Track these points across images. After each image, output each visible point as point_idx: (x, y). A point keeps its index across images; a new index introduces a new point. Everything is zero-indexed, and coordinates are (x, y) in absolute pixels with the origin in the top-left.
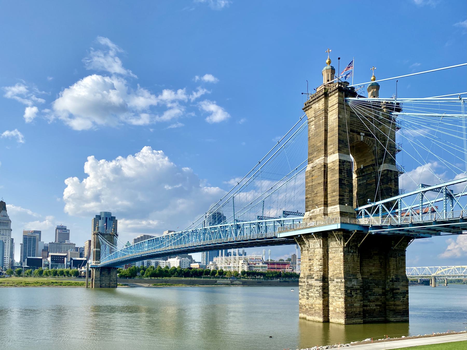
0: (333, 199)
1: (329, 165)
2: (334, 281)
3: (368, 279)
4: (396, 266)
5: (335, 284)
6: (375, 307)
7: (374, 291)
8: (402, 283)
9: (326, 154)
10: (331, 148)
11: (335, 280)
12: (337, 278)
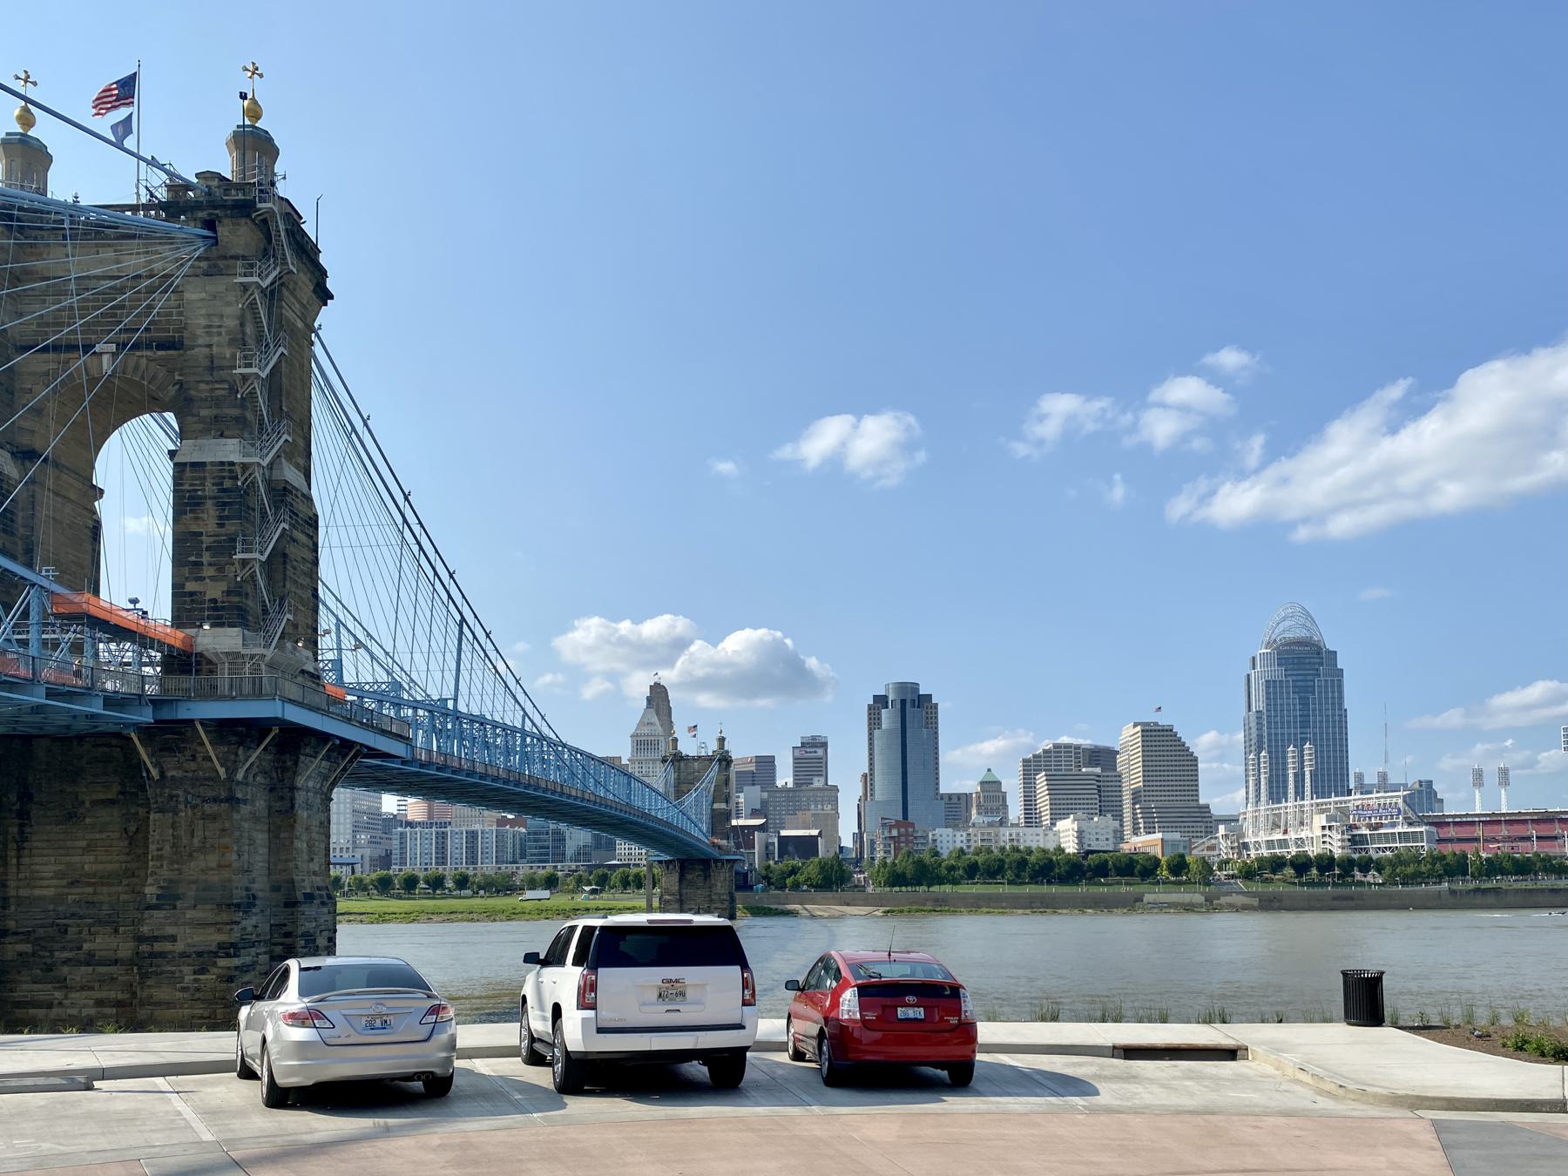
3: (59, 899)
4: (174, 845)
6: (92, 1011)
7: (86, 946)
8: (190, 914)
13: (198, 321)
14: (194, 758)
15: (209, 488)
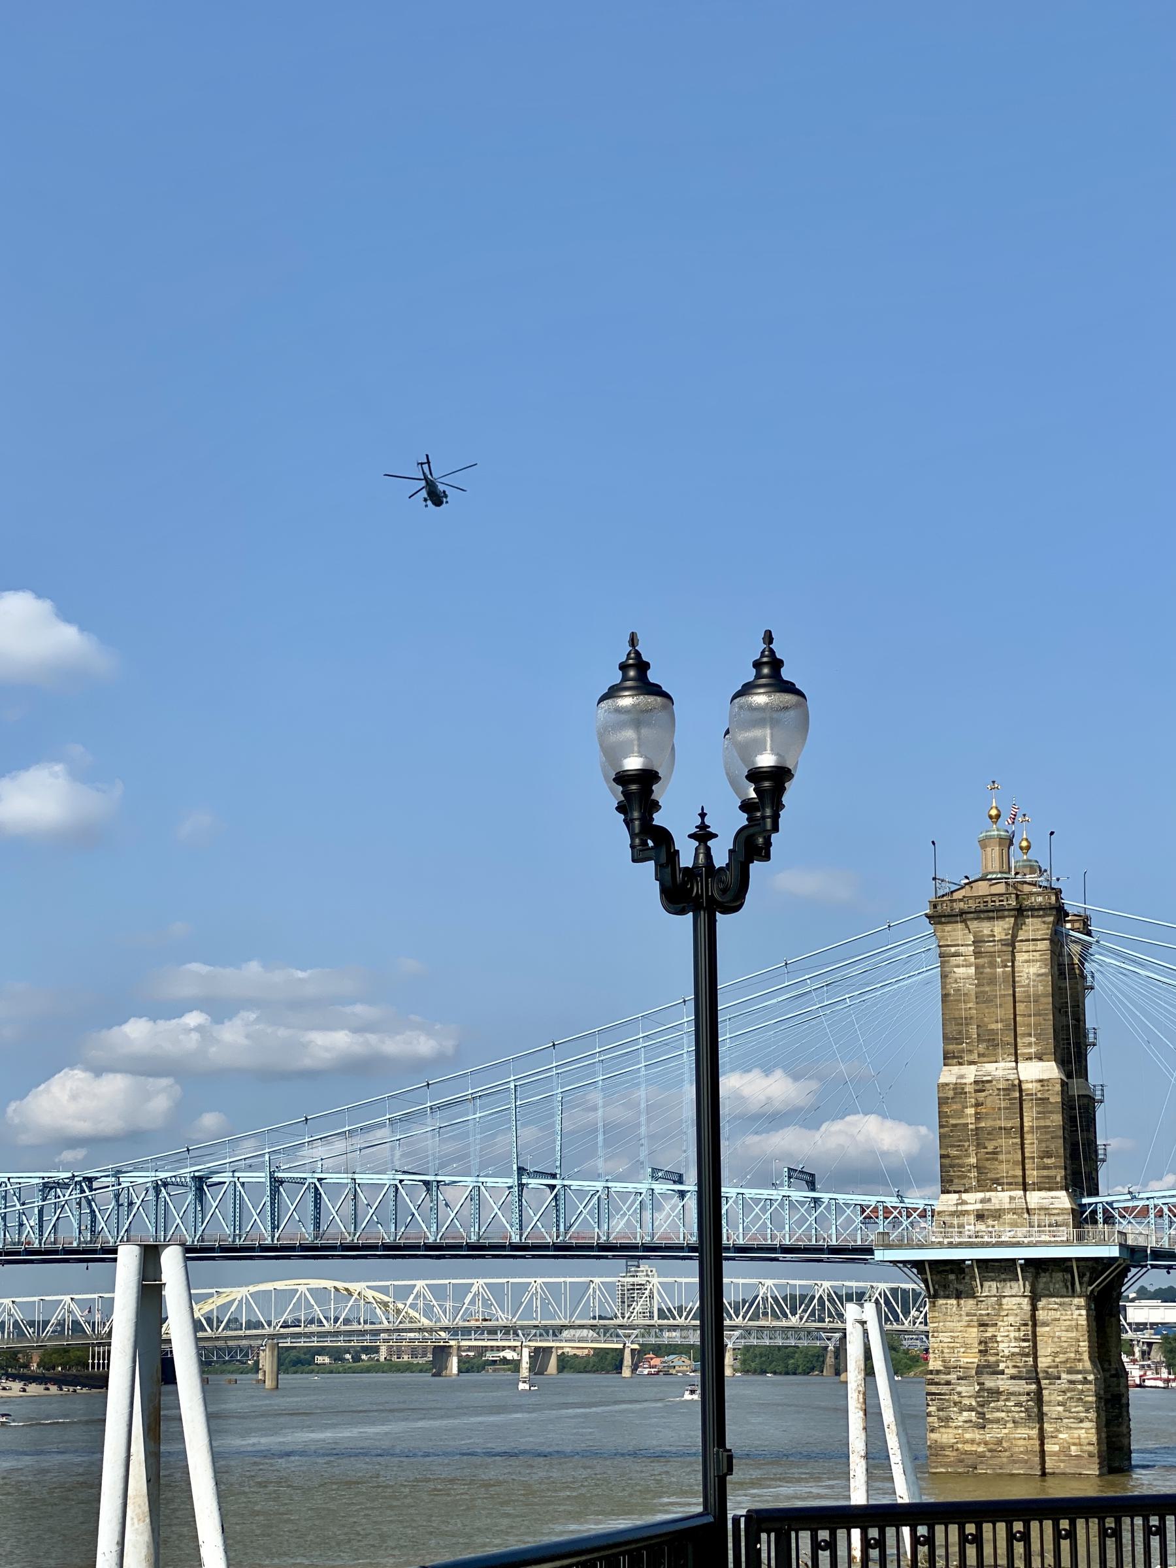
0: (1045, 1173)
1: (1024, 1086)
2: (1059, 1378)
5: (1065, 1386)
9: (1016, 1062)
10: (1030, 1045)
11: (1064, 1376)
12: (1069, 1372)
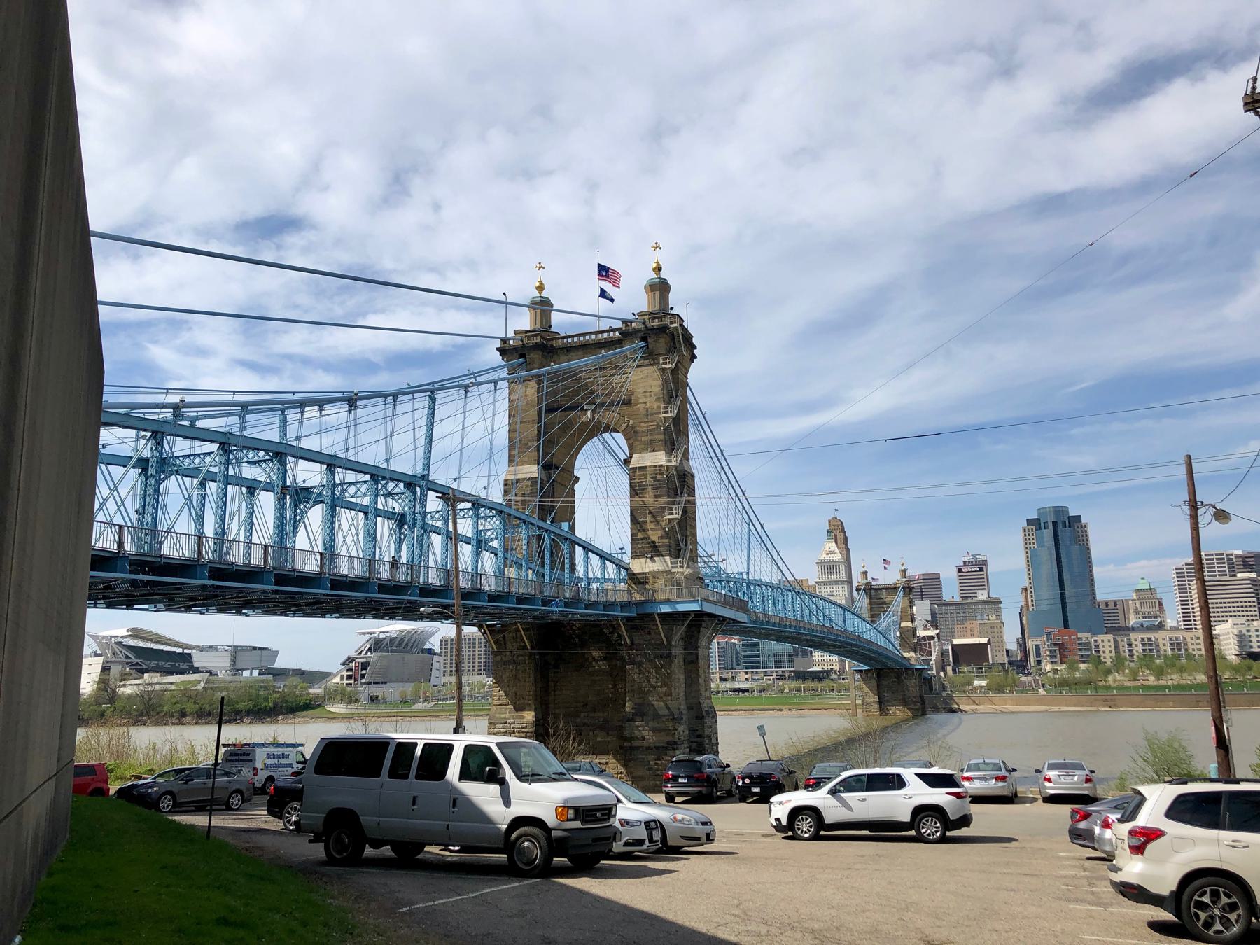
13: (639, 390)
14: (649, 633)
15: (649, 480)
